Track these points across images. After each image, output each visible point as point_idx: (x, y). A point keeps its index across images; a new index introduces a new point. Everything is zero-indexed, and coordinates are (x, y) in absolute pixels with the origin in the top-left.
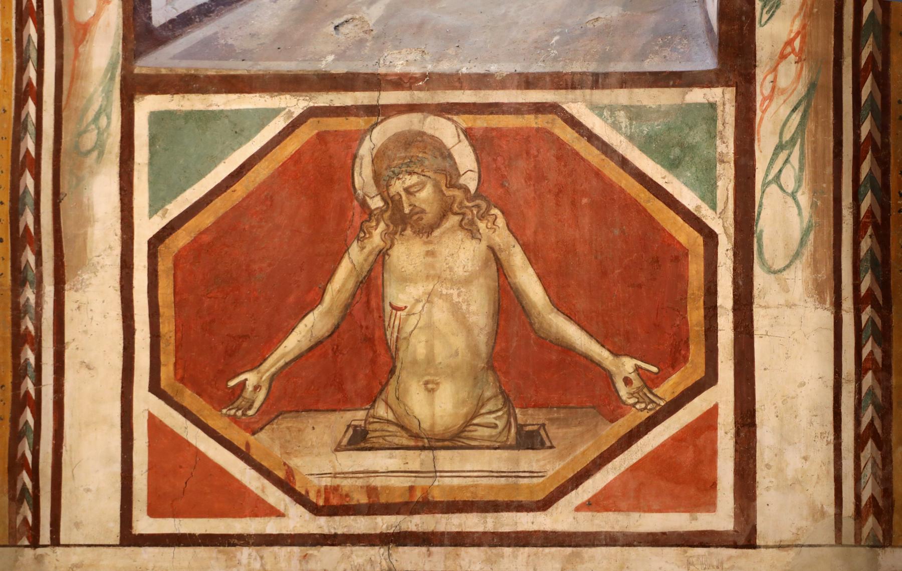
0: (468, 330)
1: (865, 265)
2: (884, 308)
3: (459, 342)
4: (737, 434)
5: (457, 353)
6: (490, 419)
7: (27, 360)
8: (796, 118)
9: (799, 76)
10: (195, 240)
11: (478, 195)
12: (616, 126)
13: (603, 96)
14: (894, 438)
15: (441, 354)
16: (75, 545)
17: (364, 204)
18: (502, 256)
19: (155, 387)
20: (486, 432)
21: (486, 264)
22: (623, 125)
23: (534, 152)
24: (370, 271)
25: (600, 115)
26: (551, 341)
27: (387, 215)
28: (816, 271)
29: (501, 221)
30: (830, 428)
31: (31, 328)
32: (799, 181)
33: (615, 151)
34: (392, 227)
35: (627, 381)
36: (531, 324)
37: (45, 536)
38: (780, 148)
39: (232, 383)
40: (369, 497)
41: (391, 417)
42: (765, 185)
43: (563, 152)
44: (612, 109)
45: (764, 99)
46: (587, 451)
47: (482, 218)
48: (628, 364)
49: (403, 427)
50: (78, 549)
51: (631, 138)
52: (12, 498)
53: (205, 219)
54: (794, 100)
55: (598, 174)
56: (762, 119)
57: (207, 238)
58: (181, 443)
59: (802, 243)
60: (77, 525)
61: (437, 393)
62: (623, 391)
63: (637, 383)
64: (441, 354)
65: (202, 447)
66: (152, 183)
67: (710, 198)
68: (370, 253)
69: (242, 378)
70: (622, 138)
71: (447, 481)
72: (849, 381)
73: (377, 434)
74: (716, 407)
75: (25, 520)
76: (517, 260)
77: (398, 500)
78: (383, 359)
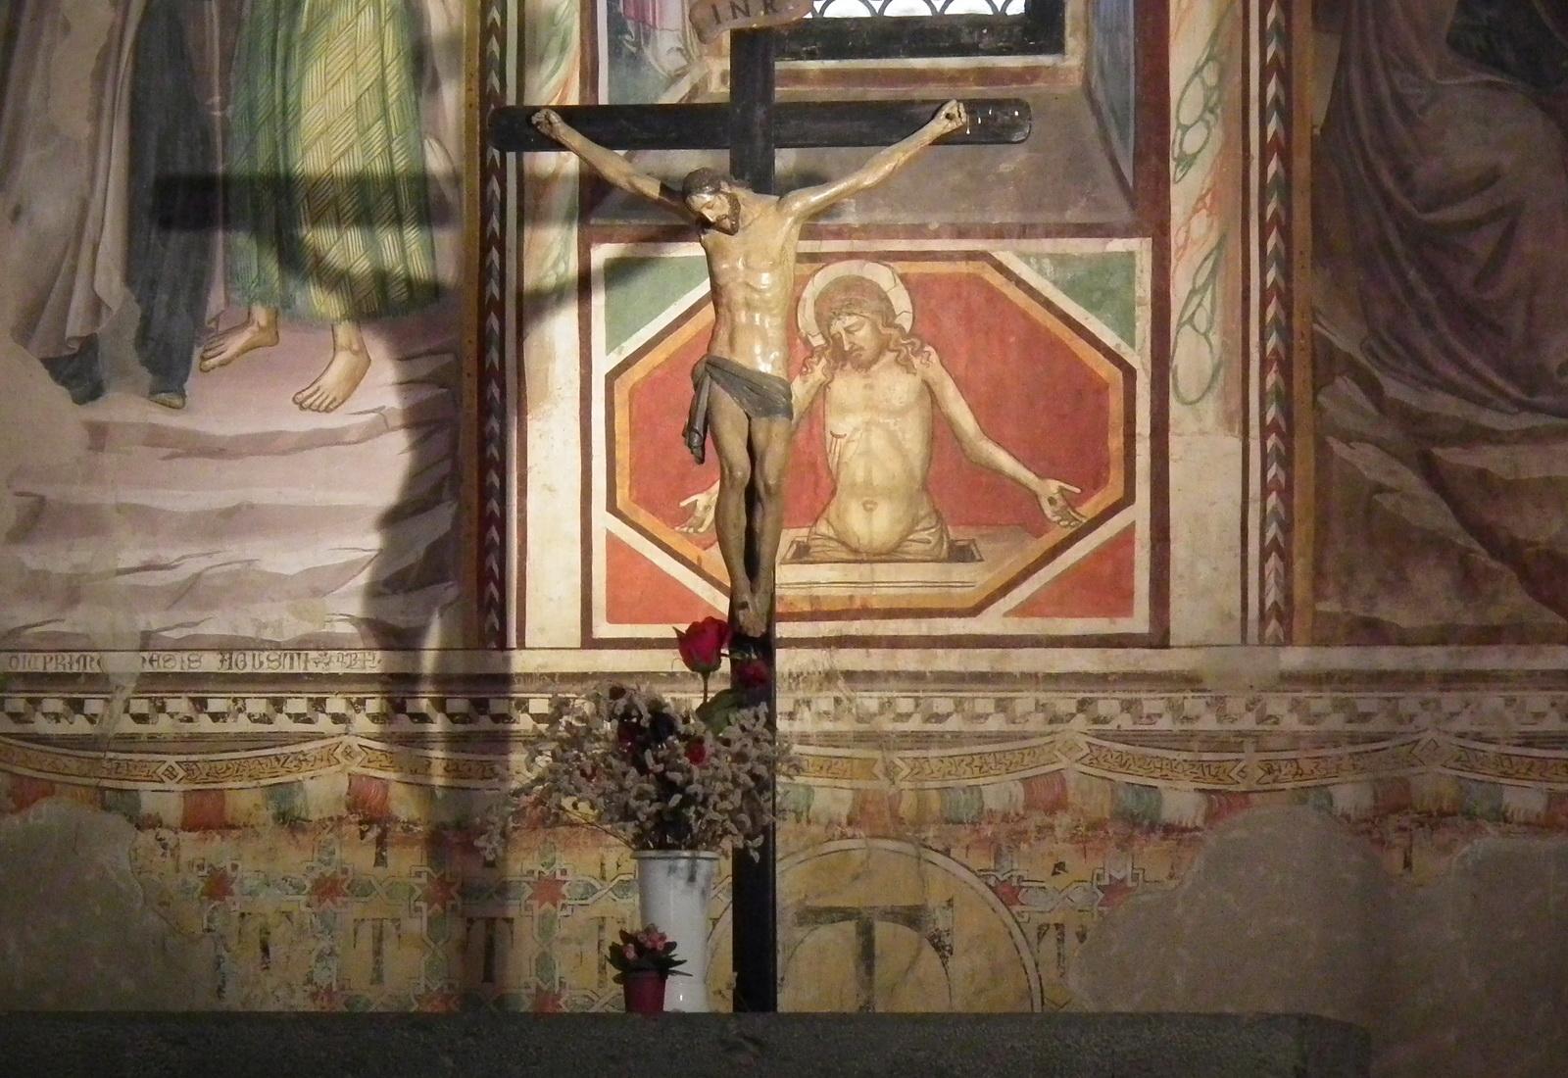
0: (904, 455)
1: (1271, 397)
2: (1287, 437)
3: (895, 466)
4: (1153, 548)
5: (894, 476)
6: (924, 535)
7: (492, 484)
8: (1209, 264)
9: (1210, 227)
10: (649, 375)
11: (912, 333)
12: (1041, 271)
13: (1030, 245)
14: (1295, 551)
15: (878, 478)
16: (540, 649)
17: (806, 342)
18: (936, 389)
19: (612, 508)
20: (921, 547)
21: (920, 396)
22: (1048, 271)
23: (965, 294)
24: (812, 403)
25: (1028, 263)
26: (982, 466)
27: (827, 352)
28: (1226, 402)
29: (934, 357)
30: (1238, 543)
31: (496, 454)
32: (1211, 322)
33: (1040, 294)
34: (832, 361)
35: (1052, 501)
36: (963, 451)
37: (513, 641)
38: (1193, 292)
39: (684, 504)
40: (812, 605)
41: (831, 533)
42: (1180, 325)
43: (993, 296)
44: (1039, 257)
45: (1178, 249)
46: (1013, 564)
47: (916, 354)
48: (1053, 486)
49: (844, 543)
50: (543, 651)
51: (1055, 283)
52: (480, 606)
53: (658, 356)
54: (1206, 250)
55: (1025, 315)
56: (1176, 267)
57: (658, 373)
58: (636, 557)
59: (1214, 377)
60: (542, 630)
61: (874, 513)
62: (1048, 510)
63: (1061, 503)
64: (878, 478)
65: (657, 562)
66: (608, 324)
67: (1127, 334)
68: (812, 386)
69: (693, 498)
70: (1048, 283)
71: (884, 591)
72: (1255, 501)
73: (819, 549)
74: (1133, 524)
75: (493, 627)
76: (950, 393)
77: (839, 608)
78: (825, 481)
